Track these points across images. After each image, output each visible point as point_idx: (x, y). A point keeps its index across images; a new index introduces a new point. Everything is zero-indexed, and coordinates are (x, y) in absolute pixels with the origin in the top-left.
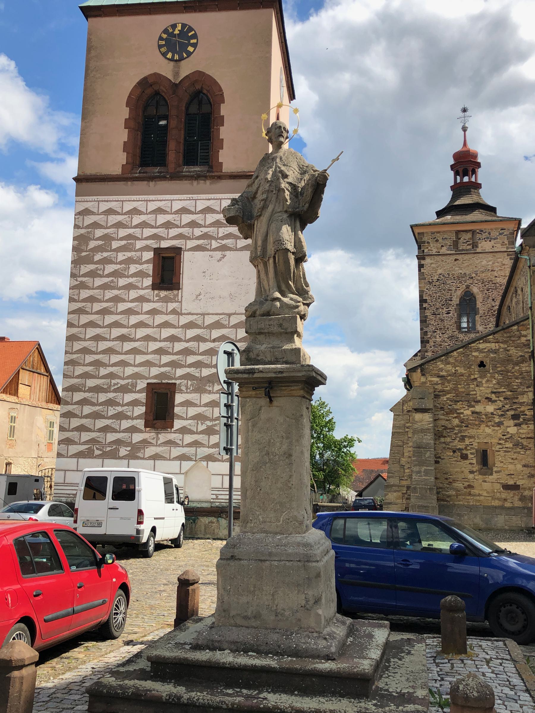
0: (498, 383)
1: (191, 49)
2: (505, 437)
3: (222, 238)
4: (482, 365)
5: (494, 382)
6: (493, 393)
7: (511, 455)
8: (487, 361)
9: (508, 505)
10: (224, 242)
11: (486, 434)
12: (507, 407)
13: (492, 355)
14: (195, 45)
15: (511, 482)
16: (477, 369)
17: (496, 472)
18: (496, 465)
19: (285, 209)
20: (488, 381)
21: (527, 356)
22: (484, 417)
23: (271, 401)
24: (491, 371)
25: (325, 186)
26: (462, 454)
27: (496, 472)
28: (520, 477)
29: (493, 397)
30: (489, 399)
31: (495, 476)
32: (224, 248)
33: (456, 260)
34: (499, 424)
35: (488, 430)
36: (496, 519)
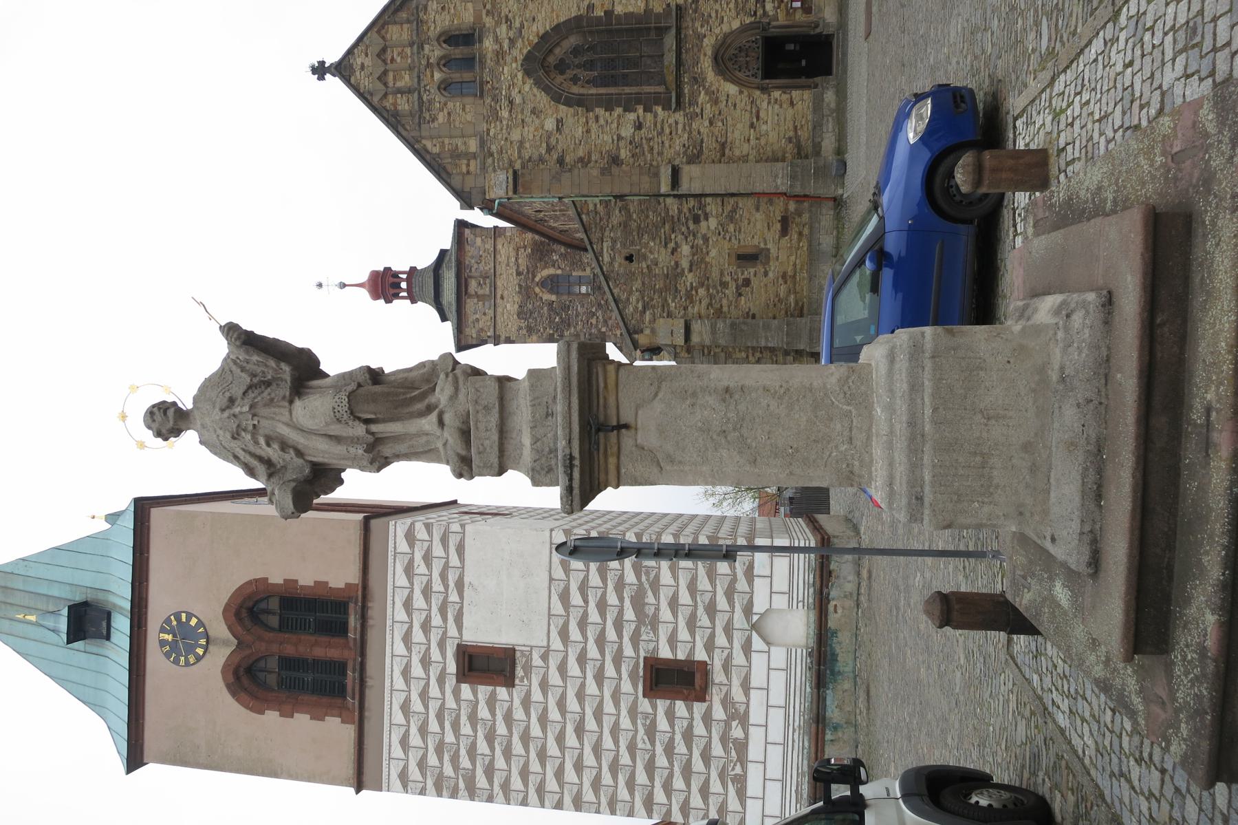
0: (654, 239)
1: (194, 622)
3: (446, 587)
4: (630, 258)
6: (666, 244)
8: (625, 252)
9: (806, 231)
10: (452, 584)
11: (718, 255)
14: (190, 616)
15: (778, 226)
16: (634, 264)
19: (287, 404)
20: (651, 252)
21: (619, 204)
23: (626, 426)
25: (252, 333)
26: (743, 285)
29: (672, 245)
30: (674, 251)
32: (460, 585)
33: (502, 298)
34: (706, 239)
35: (713, 253)
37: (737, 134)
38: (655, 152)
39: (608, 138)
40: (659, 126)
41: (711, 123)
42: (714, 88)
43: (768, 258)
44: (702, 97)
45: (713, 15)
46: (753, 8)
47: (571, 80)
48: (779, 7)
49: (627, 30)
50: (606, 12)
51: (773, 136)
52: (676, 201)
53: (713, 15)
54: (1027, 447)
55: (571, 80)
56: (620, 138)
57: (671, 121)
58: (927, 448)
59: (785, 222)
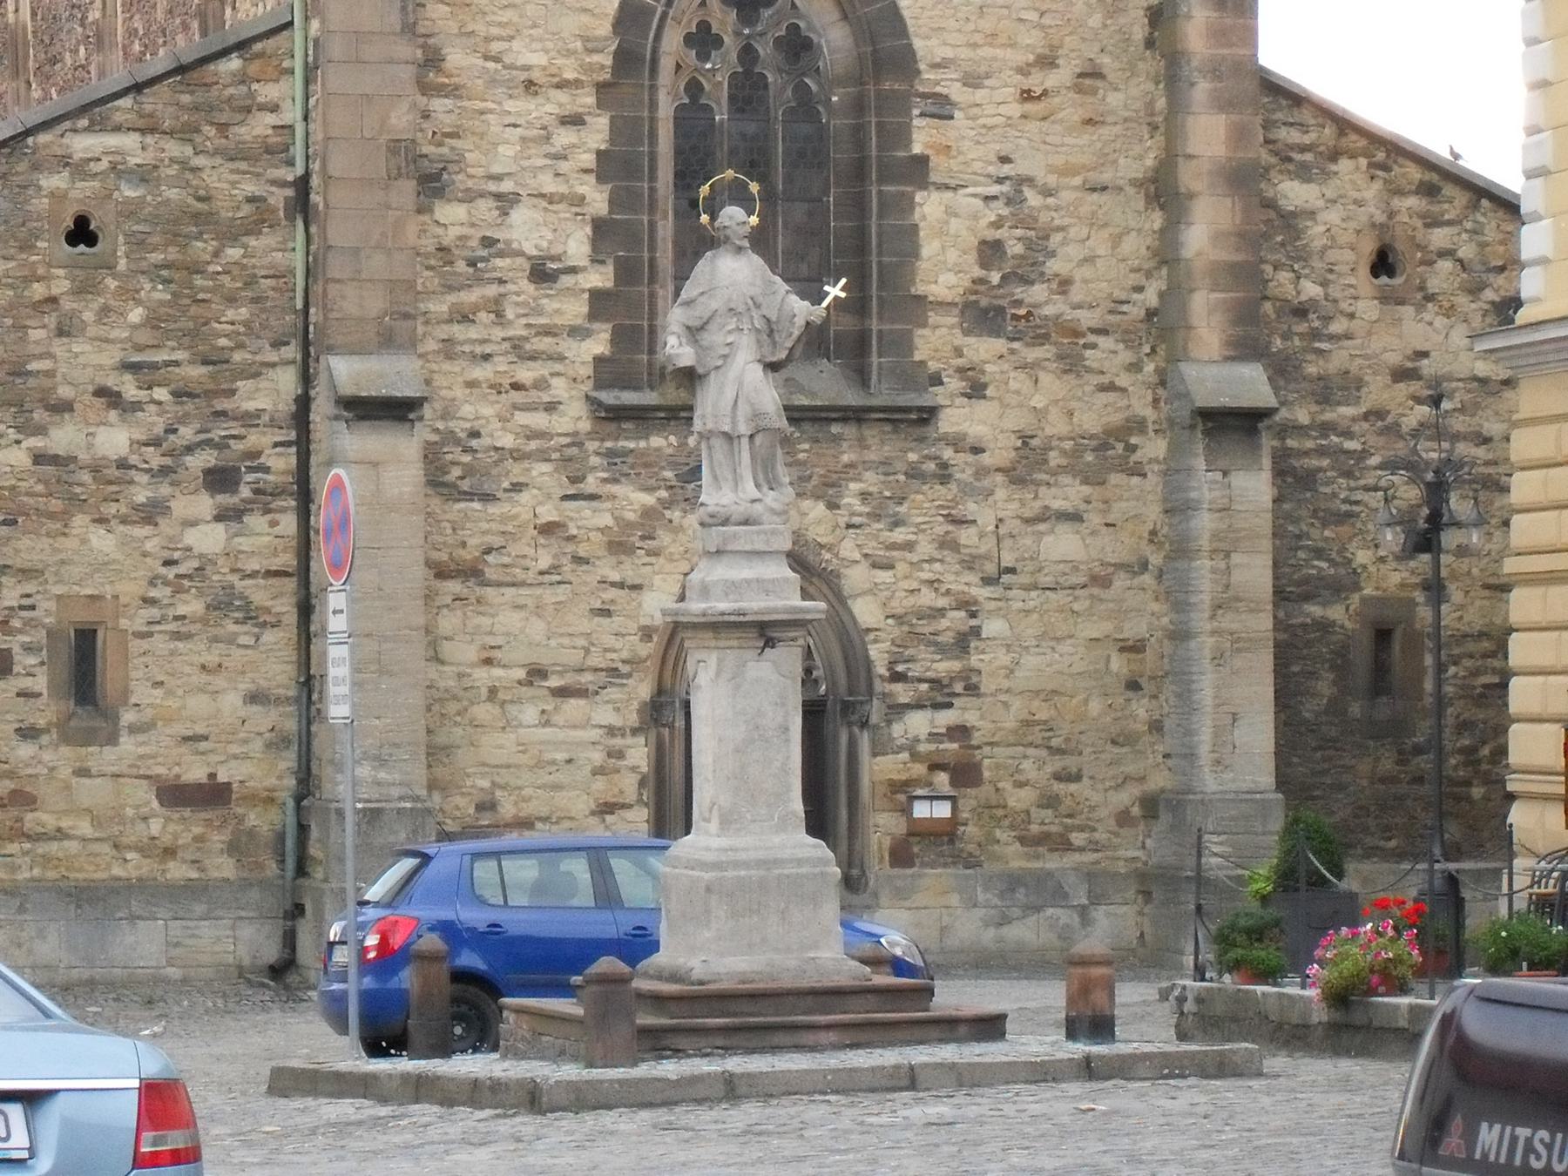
0: (153, 322)
2: (170, 573)
4: (82, 233)
5: (136, 315)
7: (200, 651)
9: (178, 871)
11: (98, 559)
12: (187, 433)
13: (130, 192)
15: (195, 773)
17: (133, 729)
18: (133, 700)
20: (105, 310)
21: (279, 198)
22: (86, 477)
24: (122, 265)
27: (133, 729)
28: (235, 749)
29: (130, 389)
30: (109, 396)
31: (127, 744)
34: (151, 513)
35: (103, 542)
36: (130, 939)
37: (509, 620)
38: (458, 331)
39: (506, 156)
40: (544, 343)
41: (548, 529)
42: (664, 538)
43: (87, 738)
44: (634, 498)
45: (900, 535)
46: (915, 670)
47: (704, 26)
48: (915, 756)
49: (862, 233)
50: (923, 161)
51: (498, 746)
52: (286, 406)
53: (900, 535)
54: (764, 940)
55: (704, 26)
56: (506, 202)
57: (559, 388)
58: (762, 873)
59: (213, 795)
